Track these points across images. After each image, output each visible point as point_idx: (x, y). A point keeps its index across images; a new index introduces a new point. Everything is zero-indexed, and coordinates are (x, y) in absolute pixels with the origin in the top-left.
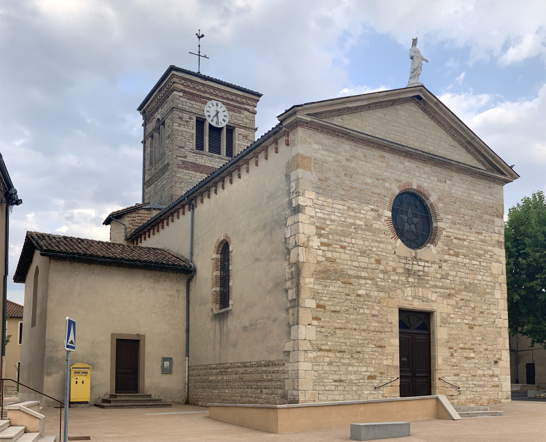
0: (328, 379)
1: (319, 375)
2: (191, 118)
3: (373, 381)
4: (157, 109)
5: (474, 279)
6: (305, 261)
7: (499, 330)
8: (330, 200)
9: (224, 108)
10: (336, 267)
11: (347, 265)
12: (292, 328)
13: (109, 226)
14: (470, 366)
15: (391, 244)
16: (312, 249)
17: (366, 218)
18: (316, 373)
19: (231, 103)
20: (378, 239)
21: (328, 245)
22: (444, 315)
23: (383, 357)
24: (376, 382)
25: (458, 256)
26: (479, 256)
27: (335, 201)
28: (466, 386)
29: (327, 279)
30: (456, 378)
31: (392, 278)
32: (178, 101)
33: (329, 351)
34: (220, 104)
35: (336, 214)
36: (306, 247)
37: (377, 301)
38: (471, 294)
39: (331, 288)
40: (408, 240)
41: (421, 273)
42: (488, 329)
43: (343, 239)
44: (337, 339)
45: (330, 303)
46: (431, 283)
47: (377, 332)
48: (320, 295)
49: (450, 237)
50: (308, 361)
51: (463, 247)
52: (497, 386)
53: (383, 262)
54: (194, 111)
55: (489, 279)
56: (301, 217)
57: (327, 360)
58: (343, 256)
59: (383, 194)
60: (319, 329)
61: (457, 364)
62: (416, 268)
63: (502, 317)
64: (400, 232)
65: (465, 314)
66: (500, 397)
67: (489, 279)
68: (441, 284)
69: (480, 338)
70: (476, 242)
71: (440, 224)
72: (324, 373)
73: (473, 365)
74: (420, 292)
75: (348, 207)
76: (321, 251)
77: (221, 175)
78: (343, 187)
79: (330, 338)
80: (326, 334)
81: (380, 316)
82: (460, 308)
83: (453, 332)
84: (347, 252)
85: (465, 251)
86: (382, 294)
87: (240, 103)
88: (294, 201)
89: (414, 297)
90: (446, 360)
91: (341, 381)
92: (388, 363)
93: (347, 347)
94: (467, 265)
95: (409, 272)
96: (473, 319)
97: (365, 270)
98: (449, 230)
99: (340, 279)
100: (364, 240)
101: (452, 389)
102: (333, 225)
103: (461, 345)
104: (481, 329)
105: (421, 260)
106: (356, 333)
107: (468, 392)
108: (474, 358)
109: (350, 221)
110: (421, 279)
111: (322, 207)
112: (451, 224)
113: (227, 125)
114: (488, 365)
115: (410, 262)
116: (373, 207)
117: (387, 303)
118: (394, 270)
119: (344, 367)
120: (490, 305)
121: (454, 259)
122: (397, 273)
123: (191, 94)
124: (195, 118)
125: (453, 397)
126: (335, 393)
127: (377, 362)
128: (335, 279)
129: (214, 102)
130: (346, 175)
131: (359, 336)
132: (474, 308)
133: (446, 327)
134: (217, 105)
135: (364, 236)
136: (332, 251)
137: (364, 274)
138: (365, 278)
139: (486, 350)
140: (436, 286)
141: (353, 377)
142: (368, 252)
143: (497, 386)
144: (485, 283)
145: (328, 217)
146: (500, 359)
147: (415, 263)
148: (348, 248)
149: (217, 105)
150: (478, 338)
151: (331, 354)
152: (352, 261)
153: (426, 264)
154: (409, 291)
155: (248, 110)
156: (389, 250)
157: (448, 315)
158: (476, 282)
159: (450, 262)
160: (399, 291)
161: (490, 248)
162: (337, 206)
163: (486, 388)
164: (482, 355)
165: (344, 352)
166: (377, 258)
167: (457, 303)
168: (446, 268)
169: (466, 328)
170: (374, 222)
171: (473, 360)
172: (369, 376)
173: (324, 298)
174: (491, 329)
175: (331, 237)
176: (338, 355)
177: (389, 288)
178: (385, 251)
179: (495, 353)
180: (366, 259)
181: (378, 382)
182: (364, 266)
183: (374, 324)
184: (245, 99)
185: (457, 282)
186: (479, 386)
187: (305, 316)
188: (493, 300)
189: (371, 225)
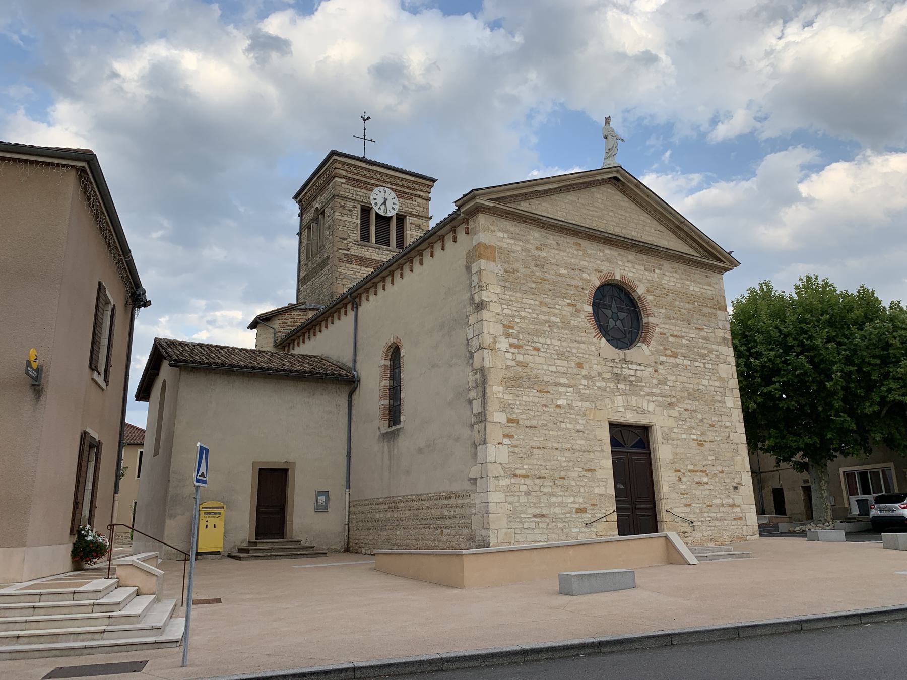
1: (515, 509)
2: (354, 207)
3: (583, 515)
4: (316, 197)
5: (698, 384)
7: (735, 447)
8: (518, 295)
9: (393, 195)
10: (530, 373)
11: (542, 369)
12: (479, 448)
13: (255, 330)
14: (704, 493)
15: (594, 344)
18: (510, 506)
21: (519, 347)
22: (666, 429)
24: (587, 517)
26: (703, 356)
29: (519, 387)
30: (688, 510)
31: (597, 384)
32: (340, 189)
34: (389, 191)
40: (614, 339)
41: (633, 379)
43: (535, 339)
44: (535, 462)
45: (524, 416)
46: (646, 390)
50: (500, 491)
53: (586, 366)
54: (358, 198)
55: (717, 384)
56: (485, 314)
57: (524, 488)
58: (537, 359)
60: (511, 449)
62: (626, 372)
63: (737, 430)
64: (604, 330)
65: (691, 428)
66: (745, 533)
67: (717, 384)
68: (658, 391)
71: (651, 320)
72: (521, 506)
73: (708, 492)
77: (390, 269)
79: (526, 460)
82: (685, 420)
84: (542, 354)
86: (587, 405)
88: (476, 297)
89: (627, 408)
90: (672, 487)
91: (543, 516)
95: (617, 378)
96: (702, 434)
99: (535, 387)
100: (561, 339)
103: (691, 467)
104: (713, 446)
105: (631, 363)
106: (557, 453)
109: (543, 318)
110: (634, 385)
111: (509, 303)
115: (619, 366)
117: (594, 414)
118: (600, 375)
119: (545, 497)
121: (672, 360)
123: (355, 180)
124: (359, 207)
125: (686, 535)
126: (536, 531)
128: (528, 387)
130: (536, 266)
132: (701, 421)
134: (385, 192)
138: (565, 386)
139: (722, 472)
140: (652, 394)
141: (557, 510)
144: (712, 388)
147: (624, 366)
149: (385, 192)
150: (710, 458)
151: (528, 481)
153: (639, 367)
154: (619, 401)
155: (421, 197)
157: (671, 429)
158: (701, 387)
160: (607, 401)
161: (715, 347)
163: (726, 522)
164: (717, 479)
165: (544, 478)
166: (578, 360)
168: (663, 372)
169: (694, 444)
171: (706, 486)
172: (577, 509)
173: (517, 411)
174: (726, 446)
175: (521, 337)
176: (537, 481)
179: (733, 476)
183: (579, 442)
184: (417, 185)
185: (678, 389)
186: (717, 519)
187: (494, 433)
189: (569, 323)
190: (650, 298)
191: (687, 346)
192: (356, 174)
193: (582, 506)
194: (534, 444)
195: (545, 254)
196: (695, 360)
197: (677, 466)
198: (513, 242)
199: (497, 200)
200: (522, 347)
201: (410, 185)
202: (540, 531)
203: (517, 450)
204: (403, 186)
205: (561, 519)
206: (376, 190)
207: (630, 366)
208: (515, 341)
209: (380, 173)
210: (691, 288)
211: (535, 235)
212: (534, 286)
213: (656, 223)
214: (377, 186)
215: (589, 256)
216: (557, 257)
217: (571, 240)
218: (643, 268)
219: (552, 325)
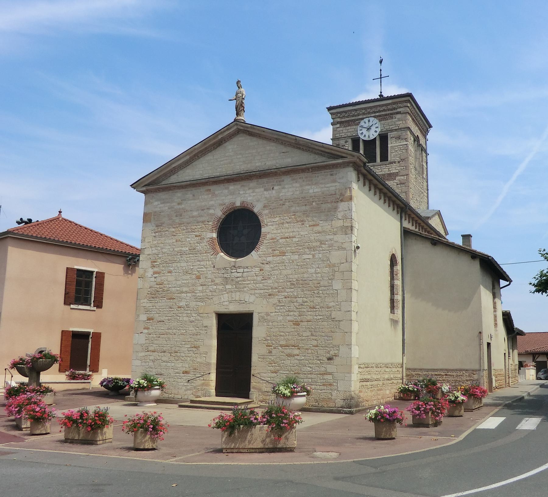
9: (376, 121)
19: (383, 113)
20: (200, 259)
21: (159, 273)
22: (262, 315)
24: (190, 376)
25: (283, 256)
26: (314, 249)
49: (275, 239)
52: (331, 385)
57: (152, 358)
67: (326, 270)
74: (237, 296)
87: (392, 110)
89: (230, 302)
95: (226, 280)
98: (275, 232)
105: (239, 267)
110: (238, 285)
113: (379, 134)
116: (197, 233)
122: (216, 284)
124: (350, 141)
129: (366, 120)
137: (185, 289)
138: (186, 292)
141: (171, 371)
147: (233, 271)
153: (246, 270)
154: (225, 297)
157: (268, 314)
158: (305, 275)
164: (310, 351)
171: (296, 357)
180: (188, 277)
190: (266, 212)
192: (347, 117)
193: (187, 370)
196: (305, 253)
199: (148, 185)
201: (389, 107)
204: (384, 110)
206: (362, 123)
207: (239, 270)
208: (156, 269)
209: (365, 108)
214: (363, 119)
217: (203, 189)
218: (263, 189)
219: (181, 253)
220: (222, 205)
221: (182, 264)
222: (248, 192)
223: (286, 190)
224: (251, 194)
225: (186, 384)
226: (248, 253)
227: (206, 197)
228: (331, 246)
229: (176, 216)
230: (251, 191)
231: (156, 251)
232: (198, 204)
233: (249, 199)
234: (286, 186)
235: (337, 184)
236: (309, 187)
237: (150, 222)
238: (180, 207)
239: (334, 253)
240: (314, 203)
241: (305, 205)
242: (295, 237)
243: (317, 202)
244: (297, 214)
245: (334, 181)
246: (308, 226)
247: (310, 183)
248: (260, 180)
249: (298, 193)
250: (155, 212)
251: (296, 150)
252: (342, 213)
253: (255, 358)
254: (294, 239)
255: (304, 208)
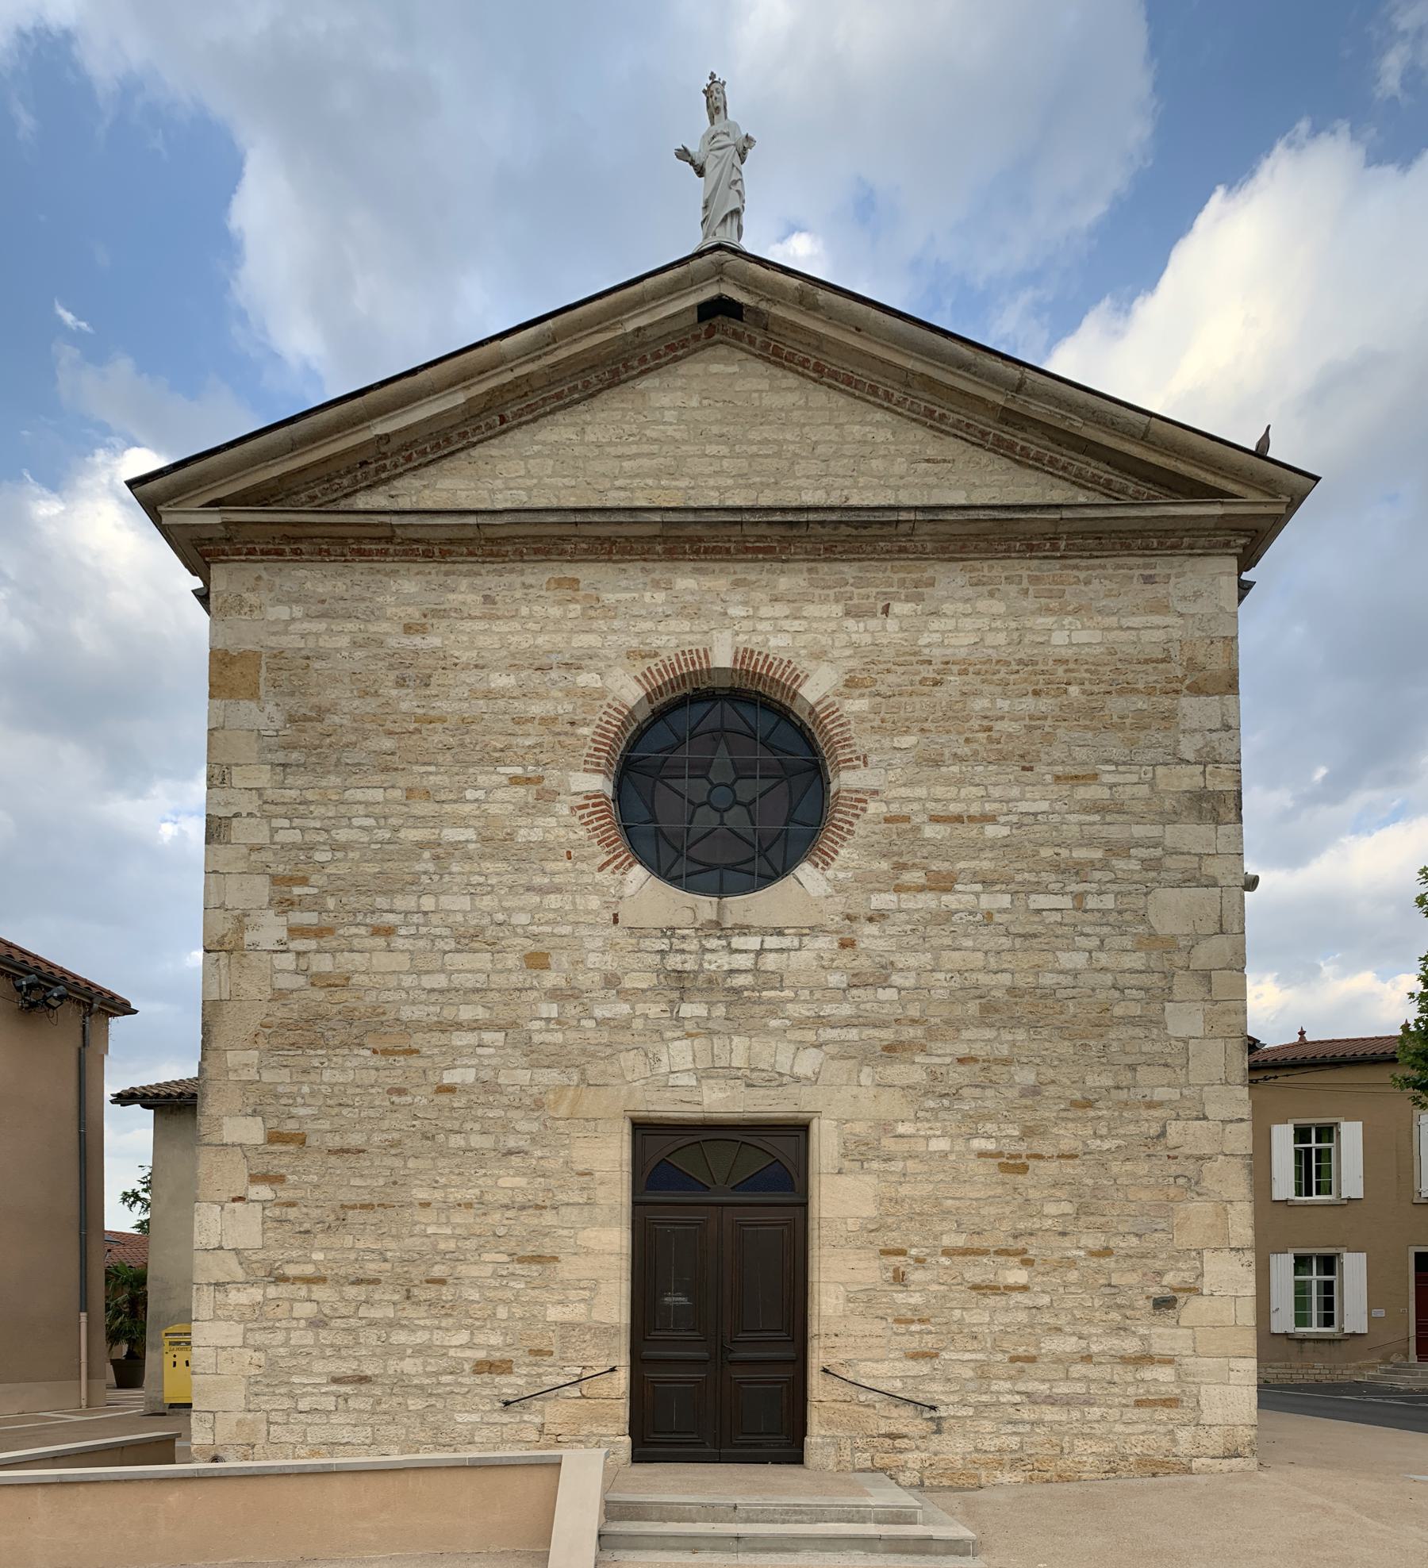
0: (306, 1372)
1: (272, 1363)
3: (499, 1380)
6: (225, 996)
7: (1191, 1167)
11: (399, 988)
14: (1002, 1318)
16: (252, 956)
17: (485, 815)
18: (259, 1357)
20: (540, 880)
21: (319, 932)
22: (859, 1128)
23: (544, 1296)
24: (511, 1385)
25: (948, 890)
26: (1079, 870)
27: (352, 780)
28: (972, 1398)
29: (312, 1045)
31: (599, 1012)
33: (308, 1280)
35: (356, 822)
36: (230, 952)
37: (528, 1101)
38: (1021, 1035)
39: (327, 1076)
41: (740, 981)
42: (1115, 1167)
43: (381, 902)
46: (794, 1010)
47: (523, 1208)
48: (284, 1101)
49: (907, 819)
50: (229, 1318)
51: (978, 848)
52: (1171, 1402)
55: (1136, 961)
57: (306, 1310)
58: (382, 961)
59: (567, 718)
61: (926, 1314)
67: (1136, 961)
68: (846, 1010)
69: (1067, 1208)
70: (1055, 818)
72: (293, 1355)
73: (1022, 1317)
74: (738, 1050)
75: (410, 792)
76: (291, 956)
78: (389, 726)
79: (321, 1239)
80: (306, 1226)
81: (539, 1153)
83: (905, 1190)
85: (986, 865)
86: (551, 1077)
89: (705, 1074)
91: (363, 1379)
92: (567, 1318)
93: (388, 1266)
94: (997, 918)
95: (680, 984)
96: (1028, 1133)
97: (476, 997)
98: (904, 792)
99: (366, 1041)
101: (895, 1412)
102: (345, 859)
103: (951, 1240)
104: (1070, 1169)
105: (744, 930)
106: (429, 1215)
107: (987, 1426)
108: (1025, 1288)
110: (743, 1002)
111: (296, 810)
112: (911, 770)
114: (1115, 1316)
116: (519, 771)
120: (1132, 1068)
121: (927, 901)
122: (623, 994)
125: (899, 1443)
126: (335, 1419)
127: (518, 1312)
128: (343, 1044)
131: (439, 1224)
132: (1034, 1091)
133: (869, 1172)
135: (476, 879)
136: (333, 952)
137: (466, 1013)
138: (475, 1027)
139: (1106, 1252)
140: (821, 1021)
141: (409, 1366)
142: (490, 933)
143: (1171, 1402)
144: (1108, 979)
145: (322, 837)
146: (1195, 1291)
147: (713, 943)
148: (403, 932)
151: (320, 1292)
152: (419, 974)
153: (772, 942)
154: (680, 1054)
156: (588, 912)
157: (885, 1127)
158: (1048, 979)
159: (903, 917)
160: (628, 1059)
162: (359, 795)
163: (1095, 1412)
164: (1073, 1276)
165: (376, 1282)
166: (531, 946)
167: (934, 1076)
170: (522, 821)
173: (302, 1111)
175: (331, 903)
176: (352, 1291)
177: (584, 1051)
178: (571, 918)
179: (1158, 1265)
180: (483, 960)
181: (521, 1382)
182: (469, 985)
185: (940, 994)
186: (1051, 1400)
188: (1158, 1047)
189: (510, 836)
190: (857, 705)
191: (1006, 844)
194: (347, 1196)
195: (436, 641)
197: (894, 1239)
198: (322, 626)
200: (330, 931)
202: (352, 1418)
203: (292, 1213)
205: (421, 1387)
208: (310, 918)
210: (1059, 638)
211: (405, 588)
212: (388, 744)
213: (921, 433)
215: (611, 613)
216: (482, 641)
218: (838, 609)
219: (442, 851)
220: (631, 654)
221: (446, 901)
222: (765, 611)
223: (950, 624)
224: (786, 624)
225: (496, 1417)
226: (778, 871)
227: (555, 612)
228: (1149, 865)
229: (401, 683)
230: (781, 609)
231: (295, 836)
232: (513, 639)
233: (773, 642)
234: (947, 607)
235: (1170, 620)
236: (1048, 621)
237: (254, 695)
238: (417, 640)
239: (1165, 895)
240: (1074, 690)
241: (1036, 693)
242: (991, 819)
243: (1087, 686)
244: (998, 726)
245: (1160, 607)
246: (1048, 778)
247: (1054, 604)
248: (824, 567)
249: (1001, 639)
250: (279, 654)
251: (985, 457)
252: (1198, 740)
253: (827, 1301)
254: (991, 831)
255: (1028, 704)
